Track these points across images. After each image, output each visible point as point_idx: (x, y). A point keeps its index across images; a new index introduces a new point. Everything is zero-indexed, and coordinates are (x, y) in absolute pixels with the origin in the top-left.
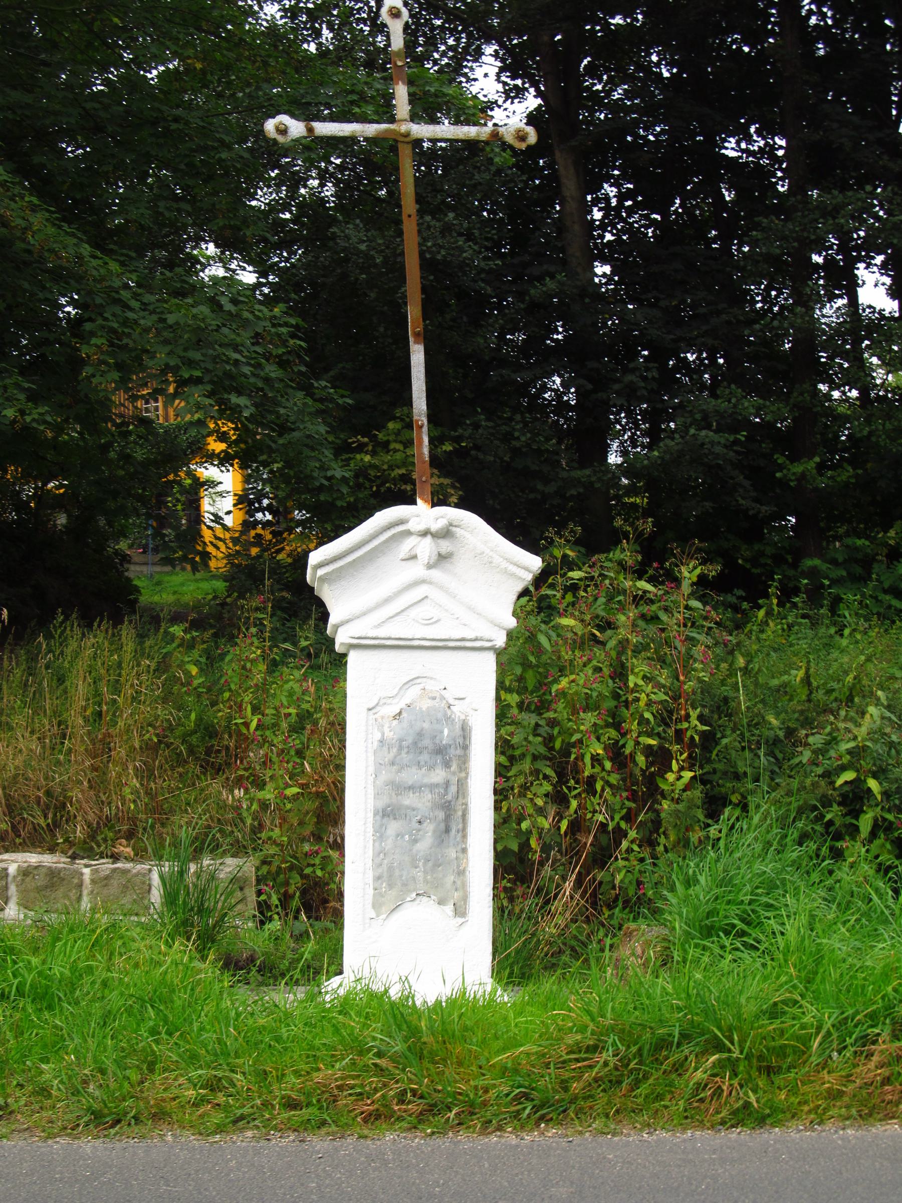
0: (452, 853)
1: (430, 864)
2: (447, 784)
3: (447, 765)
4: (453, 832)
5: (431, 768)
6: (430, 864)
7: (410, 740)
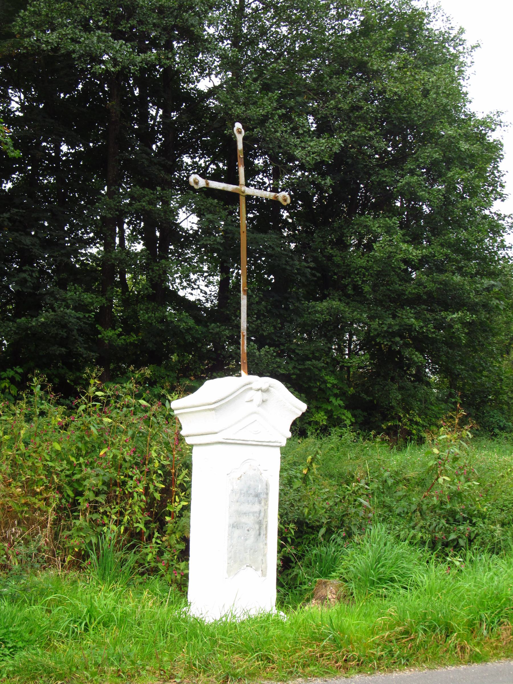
0: (261, 545)
1: (252, 551)
2: (260, 512)
3: (260, 502)
4: (262, 535)
5: (254, 504)
6: (252, 551)
7: (245, 490)
